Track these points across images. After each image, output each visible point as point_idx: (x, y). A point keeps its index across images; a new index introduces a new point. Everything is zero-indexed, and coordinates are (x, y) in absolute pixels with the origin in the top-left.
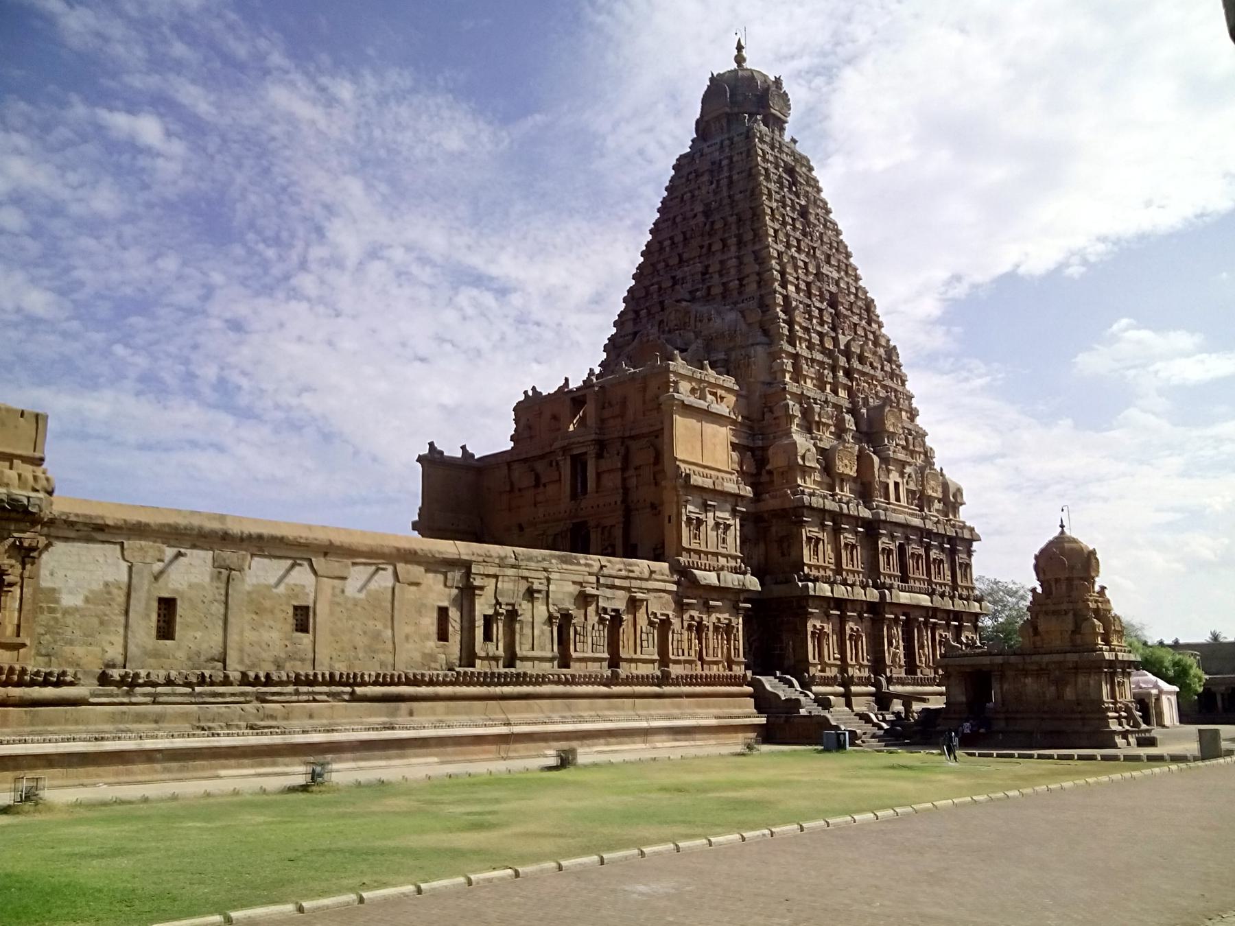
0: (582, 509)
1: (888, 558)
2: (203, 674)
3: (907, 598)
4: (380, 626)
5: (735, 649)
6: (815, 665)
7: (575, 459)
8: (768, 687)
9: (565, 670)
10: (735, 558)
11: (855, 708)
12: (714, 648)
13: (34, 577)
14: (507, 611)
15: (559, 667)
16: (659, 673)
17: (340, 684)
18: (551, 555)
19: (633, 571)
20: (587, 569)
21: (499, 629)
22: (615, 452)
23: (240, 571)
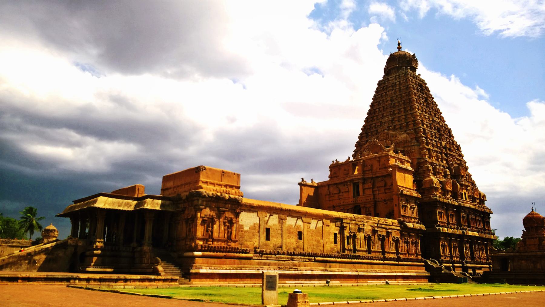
0: (358, 201)
1: (464, 219)
2: (278, 251)
3: (471, 234)
4: (319, 239)
5: (418, 250)
6: (443, 256)
7: (354, 184)
8: (429, 263)
9: (370, 255)
11: (456, 272)
13: (238, 221)
14: (353, 235)
15: (368, 254)
16: (396, 257)
17: (311, 256)
18: (364, 217)
19: (387, 223)
20: (374, 222)
22: (370, 182)
23: (285, 220)
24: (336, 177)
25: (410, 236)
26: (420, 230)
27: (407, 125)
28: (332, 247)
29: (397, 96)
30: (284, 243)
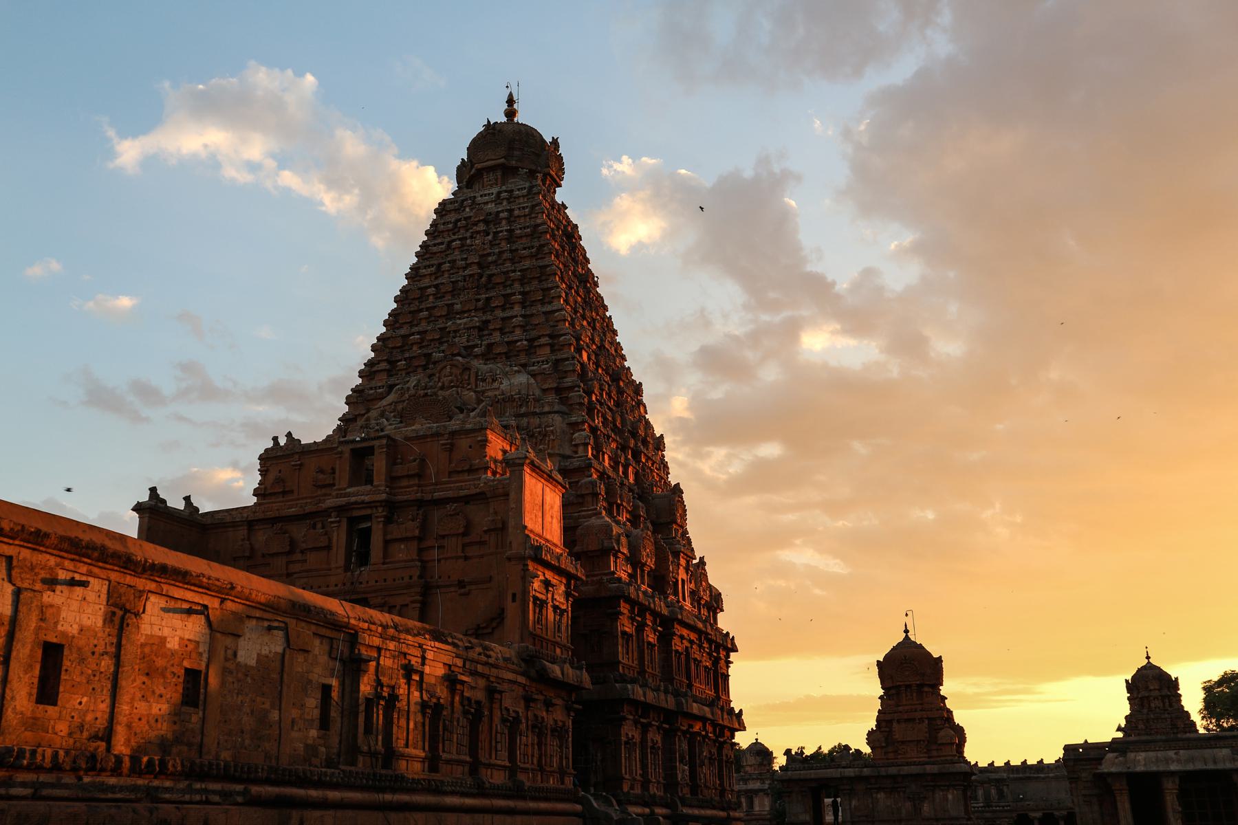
0: (361, 583)
4: (267, 706)
5: (566, 758)
7: (352, 521)
8: (595, 805)
10: (567, 649)
12: (551, 755)
14: (389, 694)
19: (489, 657)
20: (455, 650)
21: (379, 717)
22: (410, 517)
24: (284, 493)
25: (550, 709)
26: (578, 688)
27: (531, 347)
28: (310, 742)
29: (501, 253)
30: (122, 719)
